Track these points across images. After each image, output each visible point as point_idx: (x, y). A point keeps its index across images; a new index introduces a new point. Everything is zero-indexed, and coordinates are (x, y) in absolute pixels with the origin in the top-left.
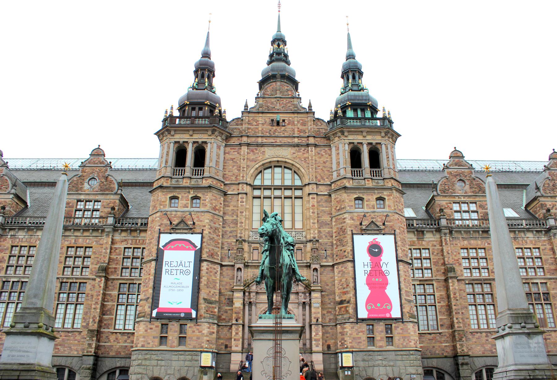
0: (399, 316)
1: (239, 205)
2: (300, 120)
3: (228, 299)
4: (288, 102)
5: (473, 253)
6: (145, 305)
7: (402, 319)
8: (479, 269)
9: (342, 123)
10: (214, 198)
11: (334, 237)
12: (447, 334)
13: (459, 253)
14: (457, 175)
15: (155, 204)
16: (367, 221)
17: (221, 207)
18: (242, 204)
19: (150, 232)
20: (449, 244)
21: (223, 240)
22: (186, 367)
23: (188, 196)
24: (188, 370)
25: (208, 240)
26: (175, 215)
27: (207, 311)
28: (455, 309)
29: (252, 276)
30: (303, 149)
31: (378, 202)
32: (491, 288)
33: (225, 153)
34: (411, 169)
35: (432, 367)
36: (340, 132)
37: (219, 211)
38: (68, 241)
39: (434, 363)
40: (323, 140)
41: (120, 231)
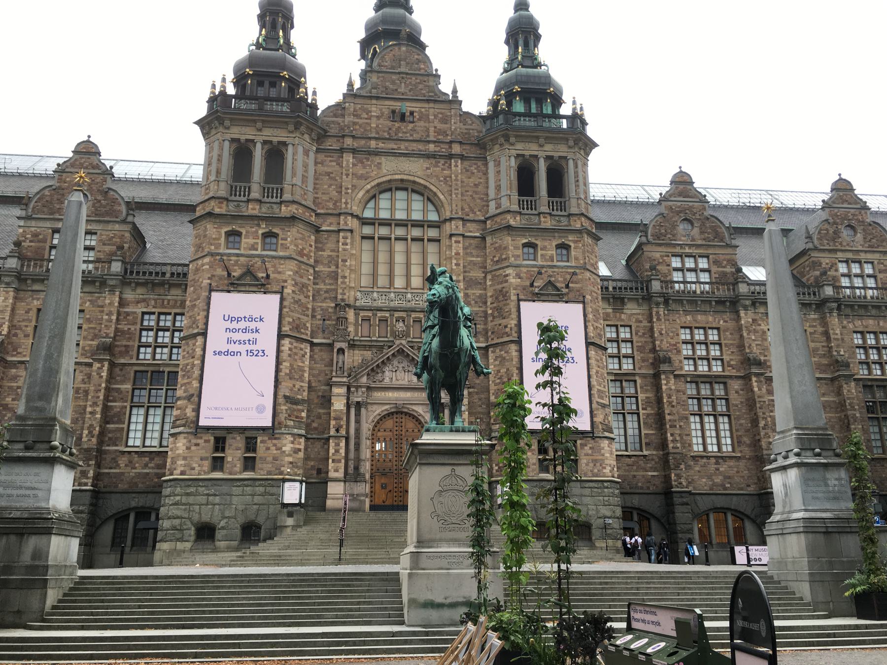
0: (588, 428)
1: (340, 249)
2: (438, 113)
3: (323, 397)
4: (418, 81)
5: (699, 335)
6: (186, 407)
7: (593, 433)
8: (708, 359)
9: (507, 121)
10: (300, 236)
11: (489, 303)
12: (655, 457)
13: (678, 335)
14: (681, 212)
15: (199, 242)
16: (541, 281)
17: (310, 251)
18: (345, 247)
19: (192, 289)
20: (663, 320)
21: (315, 304)
22: (255, 504)
23: (257, 232)
24: (258, 510)
25: (292, 303)
26: (237, 261)
27: (289, 416)
28: (670, 420)
29: (360, 361)
30: (442, 161)
31: (559, 251)
32: (726, 389)
33: (316, 163)
34: (603, 199)
35: (631, 508)
36: (503, 136)
38: (38, 299)
39: (636, 501)
40: (474, 149)
41: (133, 285)
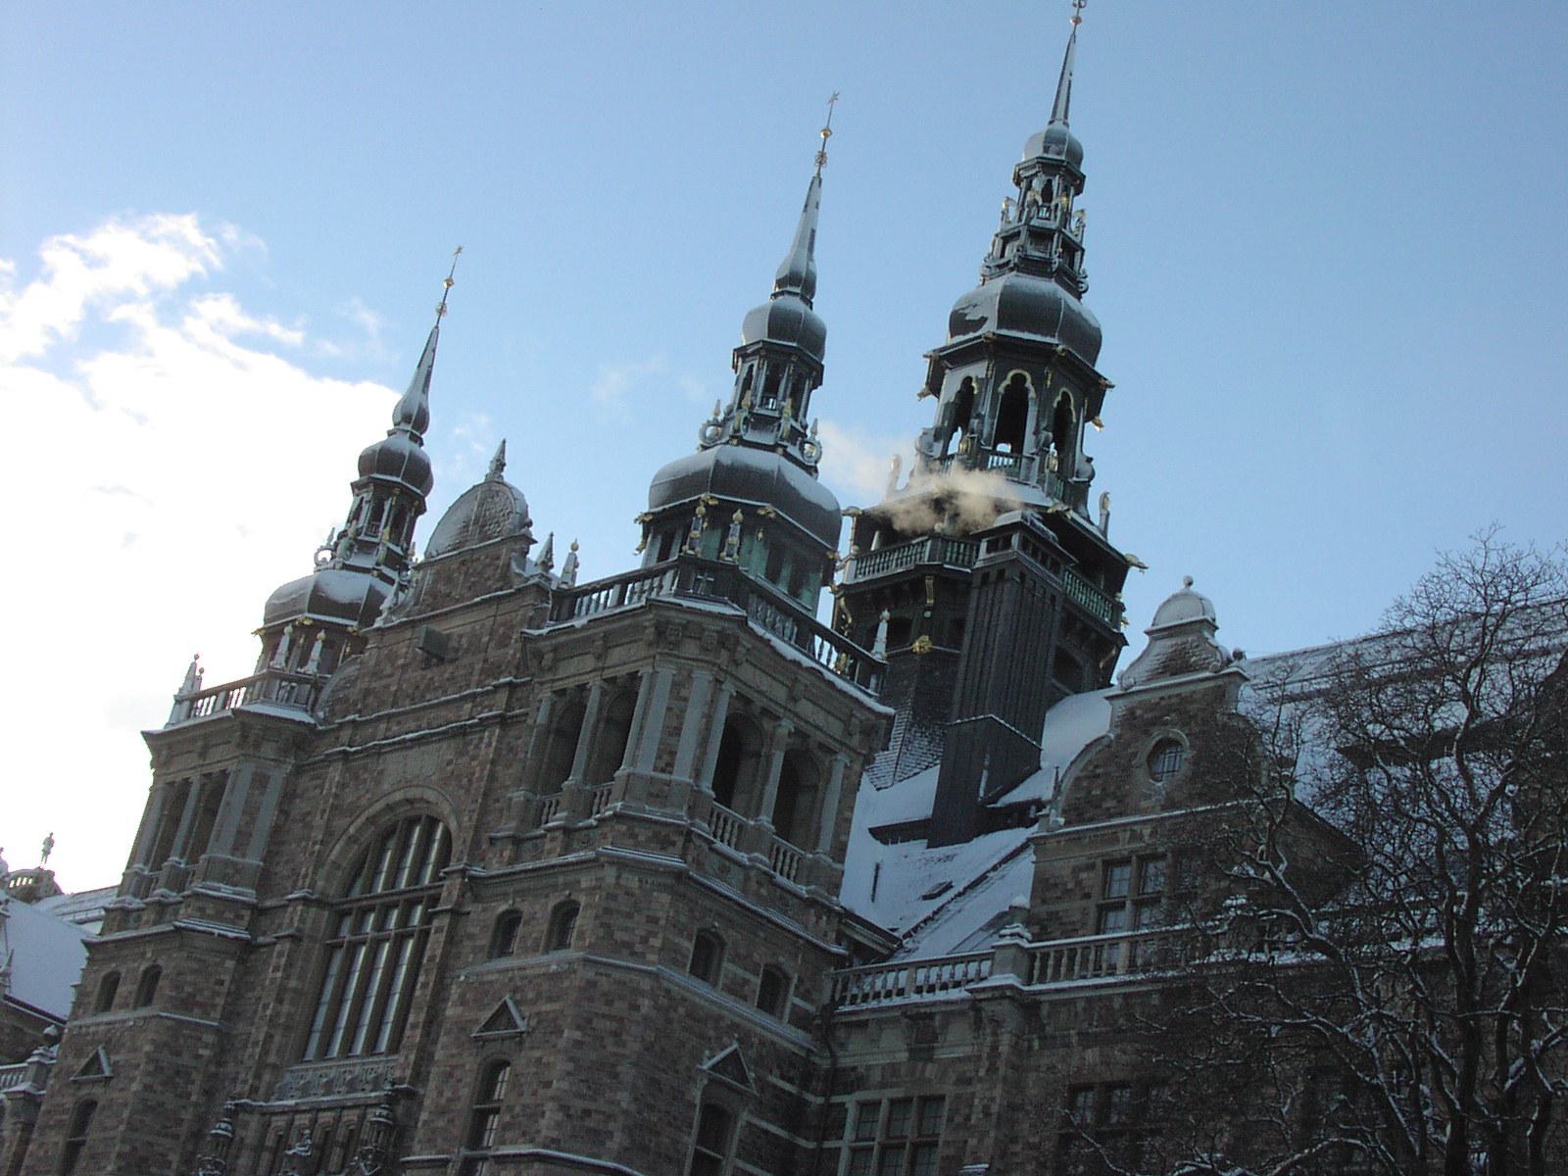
10: (195, 966)
37: (206, 1009)
